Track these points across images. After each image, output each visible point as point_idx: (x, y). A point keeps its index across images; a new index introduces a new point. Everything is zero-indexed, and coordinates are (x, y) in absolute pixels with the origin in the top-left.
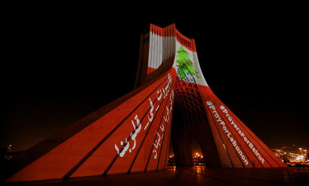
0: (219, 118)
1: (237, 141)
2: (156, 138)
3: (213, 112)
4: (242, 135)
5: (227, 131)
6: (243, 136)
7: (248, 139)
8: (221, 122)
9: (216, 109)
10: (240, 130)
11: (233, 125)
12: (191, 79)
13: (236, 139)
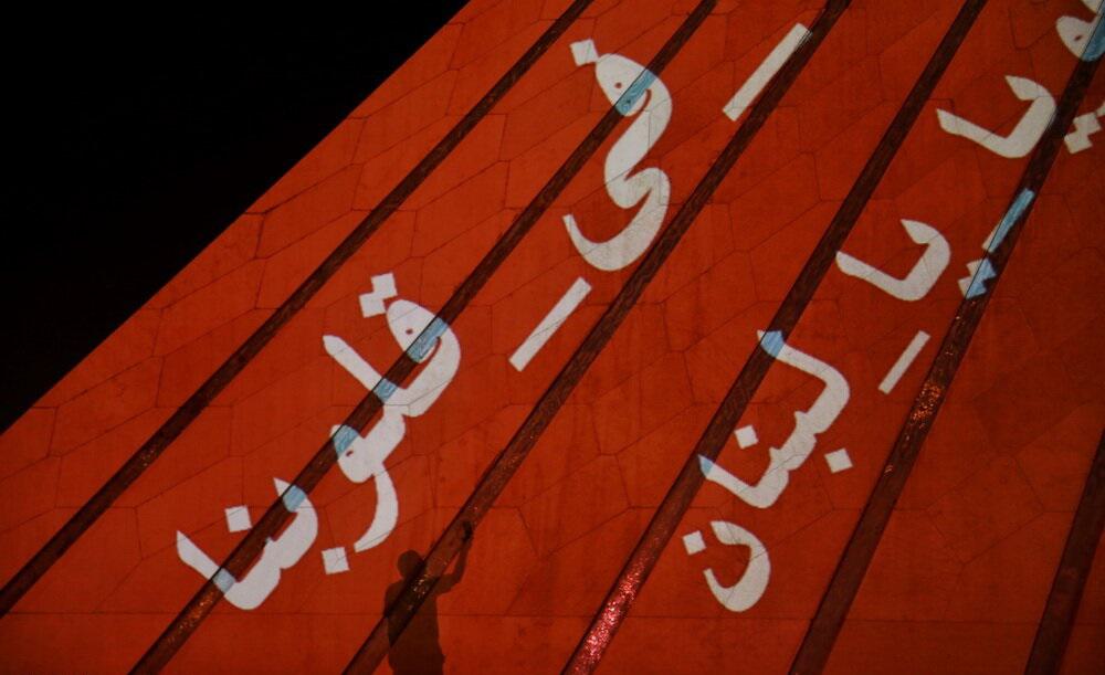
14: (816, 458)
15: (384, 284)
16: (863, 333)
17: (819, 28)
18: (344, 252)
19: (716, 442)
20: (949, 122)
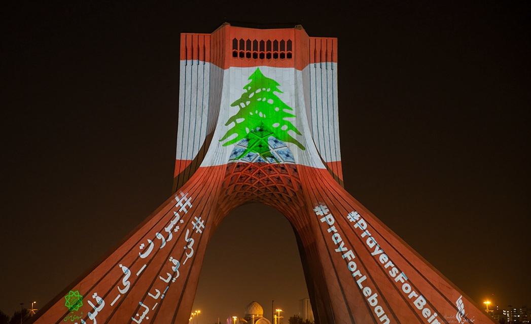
0: (343, 244)
1: (380, 293)
2: (139, 310)
3: (329, 231)
4: (400, 278)
5: (358, 273)
6: (399, 281)
7: (414, 288)
8: (346, 252)
9: (337, 224)
10: (396, 266)
11: (376, 258)
12: (286, 153)
13: (378, 289)
14: (145, 318)
15: (96, 294)
16: (151, 302)
17: (147, 266)
18: (90, 290)
19: (134, 316)
20: (161, 278)
